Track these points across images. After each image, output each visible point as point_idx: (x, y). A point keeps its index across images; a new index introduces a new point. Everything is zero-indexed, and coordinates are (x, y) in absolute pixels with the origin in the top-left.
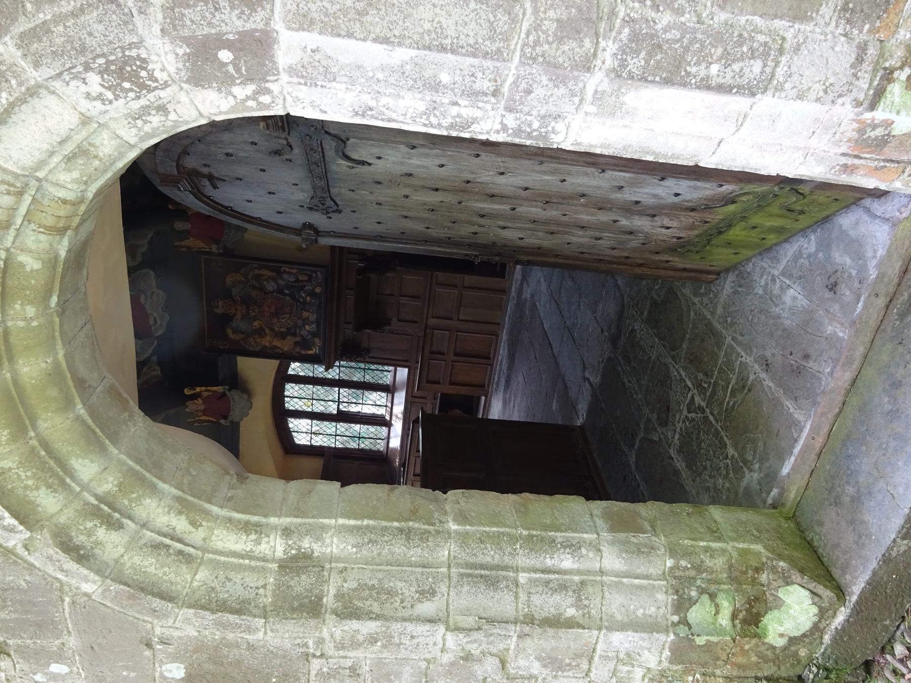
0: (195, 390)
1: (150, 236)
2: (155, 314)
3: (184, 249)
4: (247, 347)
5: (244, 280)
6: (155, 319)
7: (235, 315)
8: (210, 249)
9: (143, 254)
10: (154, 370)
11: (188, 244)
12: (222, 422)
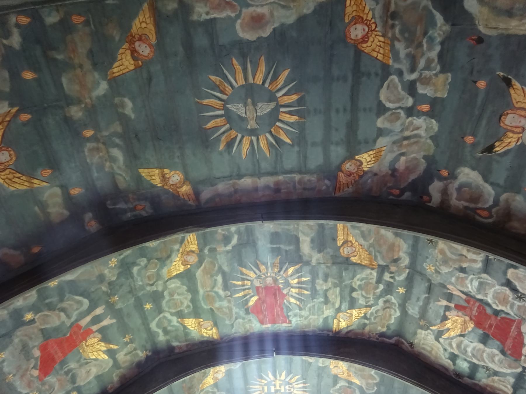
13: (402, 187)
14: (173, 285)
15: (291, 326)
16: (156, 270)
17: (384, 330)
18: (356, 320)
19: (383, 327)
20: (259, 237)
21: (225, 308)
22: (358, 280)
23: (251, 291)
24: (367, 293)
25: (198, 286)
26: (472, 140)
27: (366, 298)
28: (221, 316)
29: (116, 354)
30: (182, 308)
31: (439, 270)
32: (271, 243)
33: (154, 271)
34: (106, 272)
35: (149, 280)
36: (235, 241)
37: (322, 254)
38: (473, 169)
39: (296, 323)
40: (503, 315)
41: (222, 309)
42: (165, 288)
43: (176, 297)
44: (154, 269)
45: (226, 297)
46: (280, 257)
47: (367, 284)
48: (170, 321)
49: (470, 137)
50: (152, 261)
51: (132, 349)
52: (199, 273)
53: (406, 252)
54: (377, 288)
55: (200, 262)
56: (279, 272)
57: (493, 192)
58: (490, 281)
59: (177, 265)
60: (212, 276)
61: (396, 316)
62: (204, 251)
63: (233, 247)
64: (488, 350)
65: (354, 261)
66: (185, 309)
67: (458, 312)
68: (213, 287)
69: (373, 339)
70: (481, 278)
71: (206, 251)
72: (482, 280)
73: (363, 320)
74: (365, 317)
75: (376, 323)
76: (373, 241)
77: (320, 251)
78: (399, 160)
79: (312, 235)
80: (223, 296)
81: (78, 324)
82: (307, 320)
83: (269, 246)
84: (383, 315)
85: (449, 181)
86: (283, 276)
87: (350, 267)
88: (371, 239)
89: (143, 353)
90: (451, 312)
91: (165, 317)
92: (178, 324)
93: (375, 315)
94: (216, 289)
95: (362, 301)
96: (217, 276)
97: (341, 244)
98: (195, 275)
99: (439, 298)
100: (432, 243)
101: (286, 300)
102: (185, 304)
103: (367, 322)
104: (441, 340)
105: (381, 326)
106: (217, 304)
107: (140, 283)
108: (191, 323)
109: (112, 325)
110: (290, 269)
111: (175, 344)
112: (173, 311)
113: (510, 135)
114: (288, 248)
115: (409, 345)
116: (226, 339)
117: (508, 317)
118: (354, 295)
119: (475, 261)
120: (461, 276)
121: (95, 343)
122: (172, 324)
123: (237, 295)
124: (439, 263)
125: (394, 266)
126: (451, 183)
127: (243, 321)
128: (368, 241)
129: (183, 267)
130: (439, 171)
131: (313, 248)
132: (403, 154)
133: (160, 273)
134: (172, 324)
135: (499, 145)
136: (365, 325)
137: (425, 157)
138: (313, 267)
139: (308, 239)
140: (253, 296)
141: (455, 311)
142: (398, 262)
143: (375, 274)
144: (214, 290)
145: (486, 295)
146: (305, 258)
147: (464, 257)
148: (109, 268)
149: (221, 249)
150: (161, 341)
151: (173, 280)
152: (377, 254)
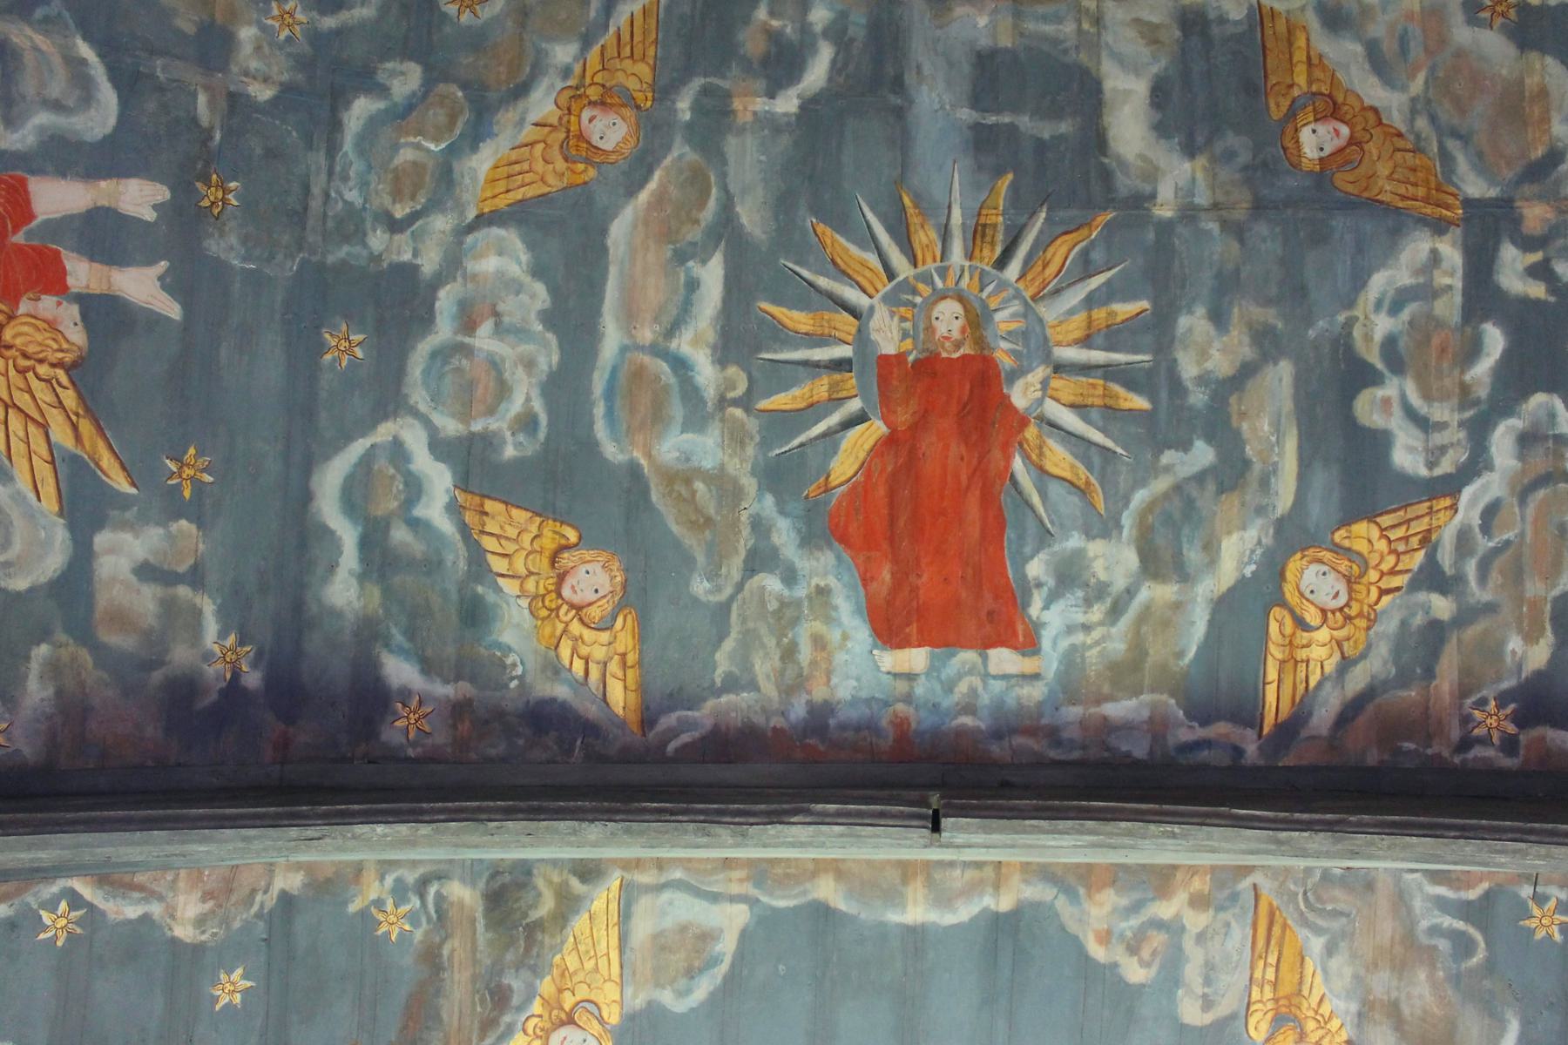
14: (489, 265)
15: (1036, 677)
16: (443, 146)
17: (1540, 655)
18: (1386, 599)
19: (1531, 638)
20: (927, 70)
21: (707, 477)
22: (1378, 305)
23: (851, 381)
24: (1427, 396)
25: (601, 300)
27: (1422, 423)
28: (675, 528)
29: (99, 523)
30: (494, 424)
32: (976, 102)
33: (432, 146)
34: (247, 33)
35: (397, 195)
36: (817, 74)
37: (1202, 161)
39: (1064, 644)
41: (688, 482)
42: (453, 265)
43: (484, 339)
44: (436, 140)
45: (723, 402)
46: (1010, 177)
47: (1424, 328)
48: (415, 488)
50: (442, 88)
51: (182, 568)
52: (620, 231)
54: (1473, 350)
55: (640, 166)
56: (1002, 263)
59: (541, 146)
60: (681, 257)
62: (674, 102)
63: (809, 106)
65: (1350, 188)
66: (508, 434)
68: (671, 331)
69: (1490, 753)
71: (684, 106)
73: (1422, 596)
74: (1432, 578)
75: (1490, 608)
76: (1426, 82)
77: (1190, 151)
79: (1155, 69)
80: (710, 394)
81: (23, 183)
82: (1125, 622)
83: (966, 114)
84: (1522, 534)
86: (1018, 295)
87: (1339, 222)
88: (1412, 76)
89: (223, 634)
91: (398, 452)
92: (446, 526)
93: (1484, 544)
94: (683, 344)
95: (1411, 449)
96: (704, 262)
97: (1284, 109)
98: (604, 231)
101: (1026, 457)
102: (516, 406)
103: (1442, 606)
105: (1520, 631)
106: (673, 445)
107: (353, 196)
108: (516, 541)
109: (155, 320)
110: (1051, 250)
111: (399, 671)
112: (450, 426)
114: (1046, 130)
116: (674, 733)
118: (1369, 408)
121: (41, 361)
122: (419, 512)
123: (781, 401)
125: (1540, 197)
127: (786, 592)
128: (1404, 88)
129: (560, 165)
131: (1161, 129)
133: (456, 165)
134: (419, 512)
136: (1436, 632)
138: (1166, 227)
139: (1140, 88)
140: (860, 419)
142: (1554, 176)
143: (1451, 252)
144: (673, 345)
146: (1125, 184)
148: (263, 28)
149: (751, 105)
150: (336, 614)
151: (496, 232)
152: (1452, 145)
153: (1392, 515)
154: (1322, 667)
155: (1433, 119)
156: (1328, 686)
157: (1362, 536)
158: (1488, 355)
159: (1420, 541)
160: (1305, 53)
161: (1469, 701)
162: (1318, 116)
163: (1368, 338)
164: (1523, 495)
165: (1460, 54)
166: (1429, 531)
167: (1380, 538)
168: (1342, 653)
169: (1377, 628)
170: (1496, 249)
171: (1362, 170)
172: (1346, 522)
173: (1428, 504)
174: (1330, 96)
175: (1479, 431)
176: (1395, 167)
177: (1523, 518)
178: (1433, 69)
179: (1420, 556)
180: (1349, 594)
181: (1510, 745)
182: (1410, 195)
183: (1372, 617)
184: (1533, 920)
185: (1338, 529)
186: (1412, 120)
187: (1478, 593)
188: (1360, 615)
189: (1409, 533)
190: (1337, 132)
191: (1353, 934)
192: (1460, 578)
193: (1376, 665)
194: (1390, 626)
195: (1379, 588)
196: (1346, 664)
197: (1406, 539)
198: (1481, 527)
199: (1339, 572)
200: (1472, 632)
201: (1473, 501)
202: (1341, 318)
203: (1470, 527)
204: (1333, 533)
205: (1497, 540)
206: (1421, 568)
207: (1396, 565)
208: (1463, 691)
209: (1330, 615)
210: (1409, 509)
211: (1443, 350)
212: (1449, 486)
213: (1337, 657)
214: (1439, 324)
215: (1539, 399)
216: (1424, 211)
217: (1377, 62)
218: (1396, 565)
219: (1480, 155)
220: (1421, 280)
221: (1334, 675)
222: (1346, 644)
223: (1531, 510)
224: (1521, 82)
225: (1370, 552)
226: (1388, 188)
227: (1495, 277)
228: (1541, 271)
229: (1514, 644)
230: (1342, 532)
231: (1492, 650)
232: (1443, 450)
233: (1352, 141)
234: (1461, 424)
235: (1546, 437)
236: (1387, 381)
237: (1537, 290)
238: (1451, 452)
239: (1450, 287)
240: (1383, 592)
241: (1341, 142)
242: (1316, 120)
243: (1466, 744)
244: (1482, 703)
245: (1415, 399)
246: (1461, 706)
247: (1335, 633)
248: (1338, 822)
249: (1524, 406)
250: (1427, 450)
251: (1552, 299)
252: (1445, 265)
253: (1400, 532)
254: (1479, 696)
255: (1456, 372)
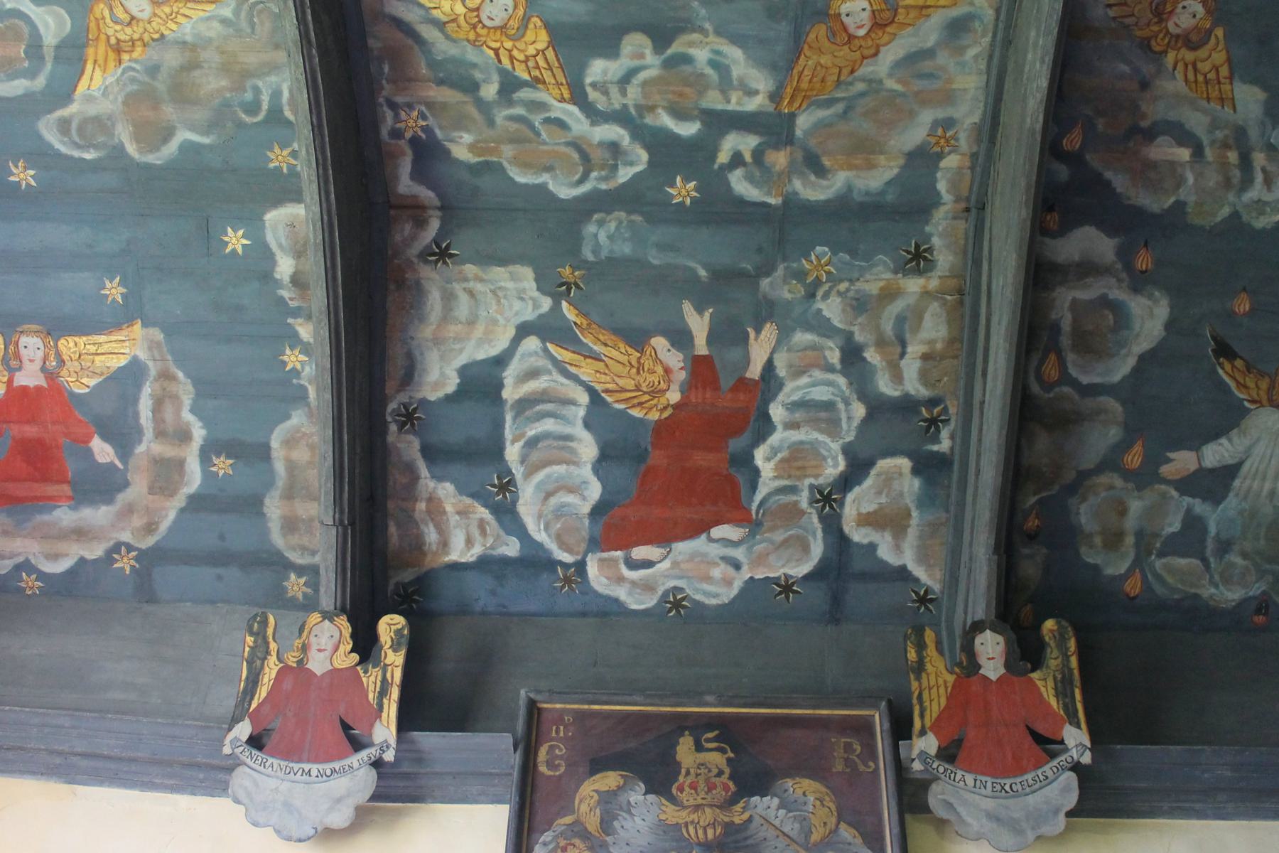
0: (395, 648)
1: (920, 572)
2: (666, 565)
3: (912, 655)
4: (547, 836)
5: (815, 837)
6: (648, 564)
7: (673, 800)
8: (923, 733)
9: (872, 547)
10: (469, 542)
11: (929, 667)
12: (244, 729)
13: (1088, 157)
18: (491, 53)
19: (472, 148)
22: (717, 52)
24: (645, 84)
26: (1242, 310)
27: (625, 80)
31: (820, 293)
38: (1169, 326)
40: (741, 479)
47: (699, 83)
49: (1247, 308)
53: (850, 188)
54: (680, 114)
57: (1116, 378)
58: (849, 427)
61: (551, 187)
64: (587, 472)
65: (812, 36)
67: (682, 368)
70: (847, 403)
72: (841, 406)
73: (496, 77)
74: (509, 86)
75: (491, 123)
76: (895, 91)
78: (1181, 144)
84: (545, 143)
85: (1124, 275)
87: (784, 28)
88: (899, 81)
90: (673, 350)
93: (537, 120)
95: (605, 72)
99: (711, 310)
100: (911, 260)
103: (490, 91)
104: (532, 343)
105: (477, 142)
113: (1264, 384)
115: (428, 247)
117: (744, 491)
119: (897, 377)
120: (827, 353)
124: (848, 290)
125: (792, 163)
126: (1119, 280)
128: (890, 75)
130: (1146, 245)
132: (1198, 152)
135: (1237, 368)
136: (472, 87)
137: (1180, 205)
141: (684, 361)
143: (752, 105)
145: (792, 425)
147: (899, 350)
152: (840, 107)
153: (555, 59)
154: (435, 8)
155: (862, 95)
156: (422, 12)
157: (538, 39)
158: (677, 125)
159: (537, 77)
160: (932, 4)
161: (423, 108)
162: (876, 13)
163: (691, 44)
164: (575, 145)
165: (912, 114)
166: (544, 82)
167: (536, 50)
168: (447, 22)
169: (469, 48)
170: (756, 133)
171: (827, 44)
172: (547, 26)
173: (564, 82)
174: (893, 22)
175: (621, 117)
176: (826, 68)
177: (558, 144)
178: (903, 95)
179: (526, 76)
180: (493, 28)
181: (397, 134)
182: (802, 77)
183: (477, 43)
184: (279, 151)
185: (541, 20)
186: (863, 80)
187: (501, 115)
188: (478, 35)
189: (542, 70)
190: (861, 27)
191: (240, 37)
192: (511, 103)
193: (441, 46)
194: (471, 55)
195: (499, 48)
196: (440, 25)
197: (537, 67)
198: (550, 118)
199: (509, 20)
200: (473, 111)
201: (570, 114)
202: (707, 26)
203: (549, 110)
204: (537, 16)
205: (540, 127)
206: (516, 77)
207: (517, 60)
208: (430, 105)
209: (475, 14)
210: (560, 70)
211: (681, 95)
212: (578, 96)
213: (445, 19)
214: (701, 94)
215: (644, 156)
216: (789, 87)
217: (913, 58)
218: (517, 60)
219: (830, 125)
220: (735, 83)
221: (430, 17)
222: (454, 25)
223: (563, 149)
224: (881, 153)
225: (526, 43)
226: (810, 63)
227: (734, 131)
228: (737, 160)
229: (467, 138)
230: (539, 23)
231: (461, 123)
232: (606, 93)
233: (851, 38)
234: (625, 106)
235: (615, 159)
236: (657, 57)
237: (723, 157)
238: (604, 98)
239: (728, 102)
240: (496, 51)
241: (852, 30)
242: (873, 12)
243: (393, 106)
244: (424, 118)
245: (643, 75)
246: (420, 103)
247: (462, 17)
248: (309, 42)
249: (638, 146)
250: (605, 82)
251: (716, 167)
252: (746, 99)
253: (542, 63)
254: (428, 115)
255: (665, 104)
